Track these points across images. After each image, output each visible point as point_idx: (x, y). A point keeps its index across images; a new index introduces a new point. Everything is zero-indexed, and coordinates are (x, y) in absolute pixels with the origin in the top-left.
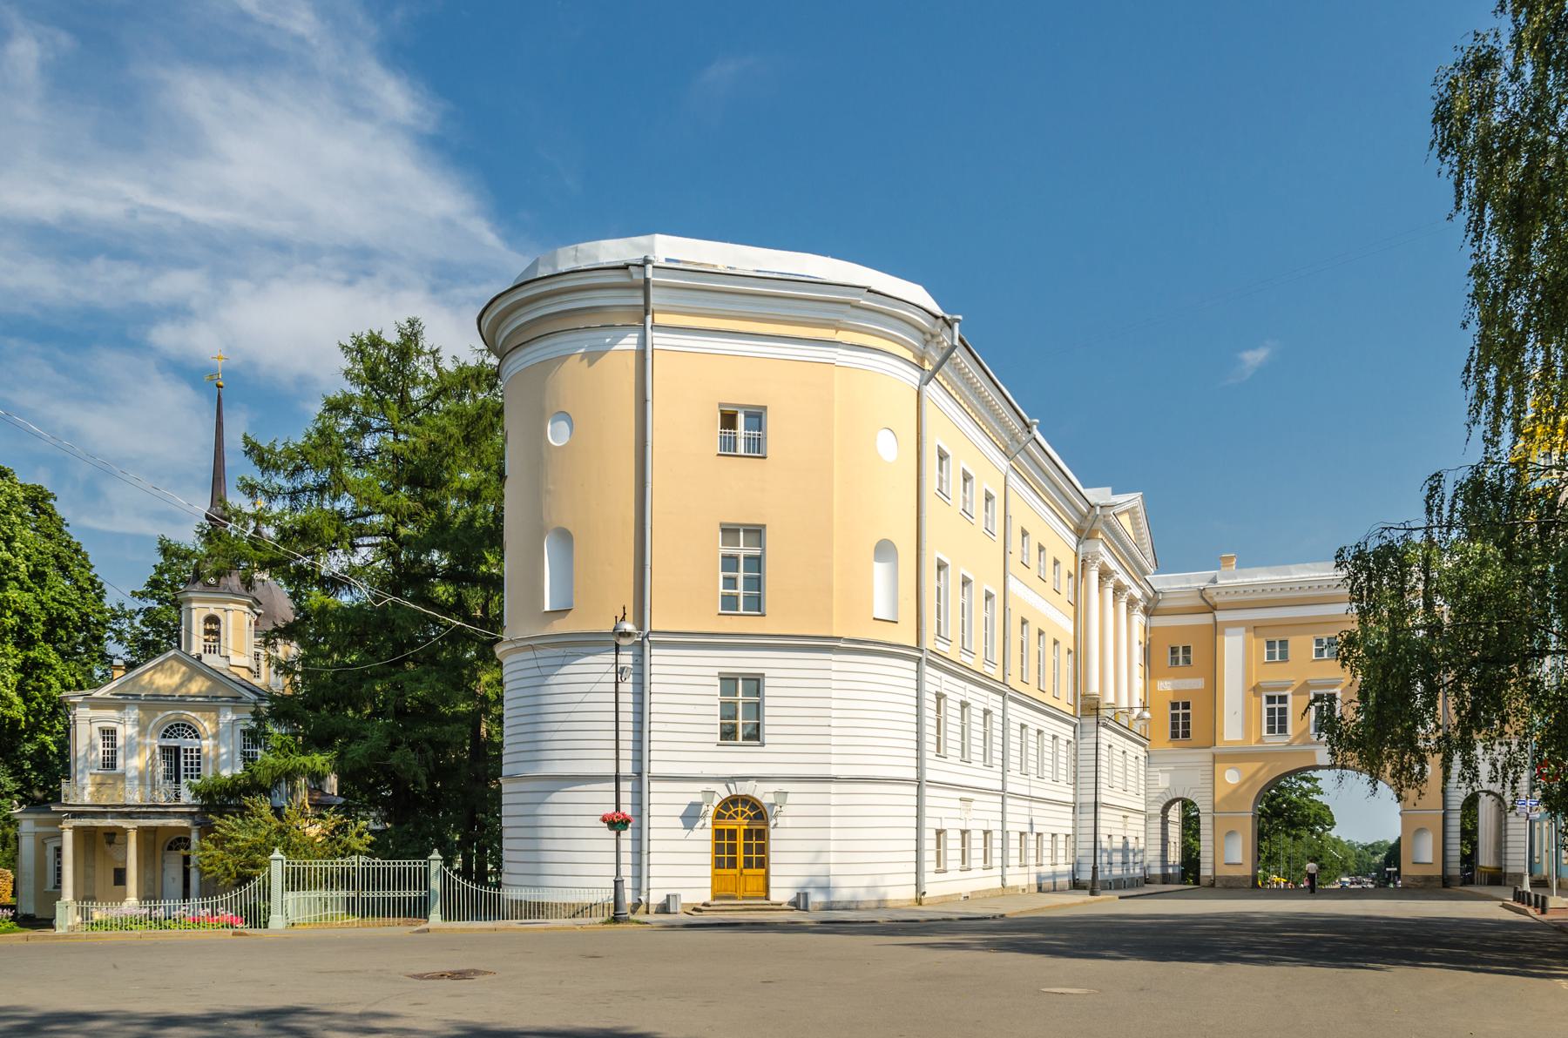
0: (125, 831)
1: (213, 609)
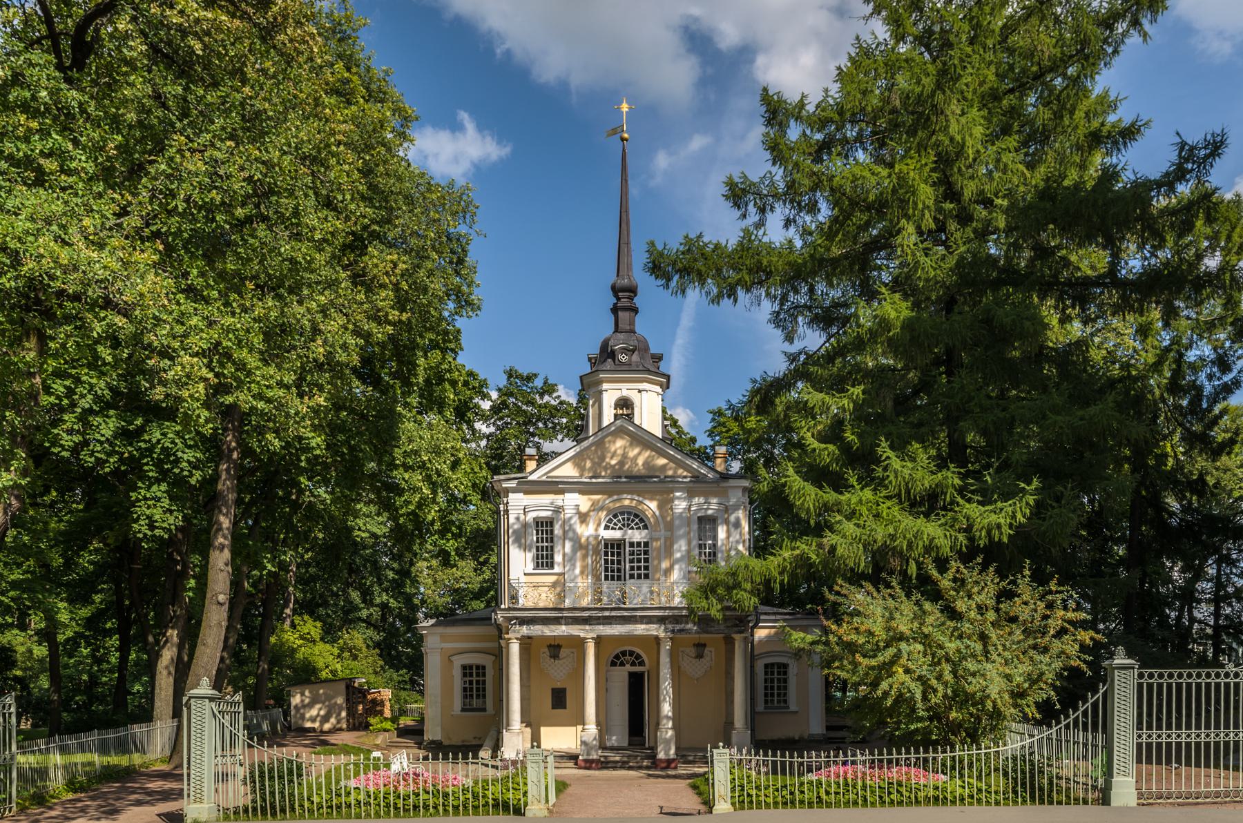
0: (580, 643)
1: (626, 390)
